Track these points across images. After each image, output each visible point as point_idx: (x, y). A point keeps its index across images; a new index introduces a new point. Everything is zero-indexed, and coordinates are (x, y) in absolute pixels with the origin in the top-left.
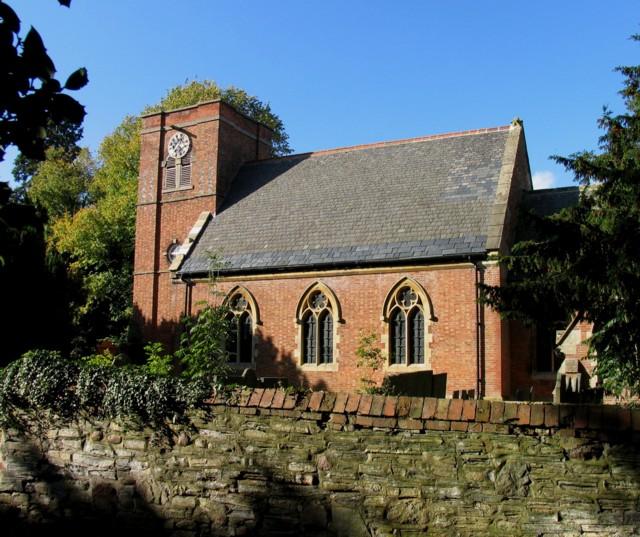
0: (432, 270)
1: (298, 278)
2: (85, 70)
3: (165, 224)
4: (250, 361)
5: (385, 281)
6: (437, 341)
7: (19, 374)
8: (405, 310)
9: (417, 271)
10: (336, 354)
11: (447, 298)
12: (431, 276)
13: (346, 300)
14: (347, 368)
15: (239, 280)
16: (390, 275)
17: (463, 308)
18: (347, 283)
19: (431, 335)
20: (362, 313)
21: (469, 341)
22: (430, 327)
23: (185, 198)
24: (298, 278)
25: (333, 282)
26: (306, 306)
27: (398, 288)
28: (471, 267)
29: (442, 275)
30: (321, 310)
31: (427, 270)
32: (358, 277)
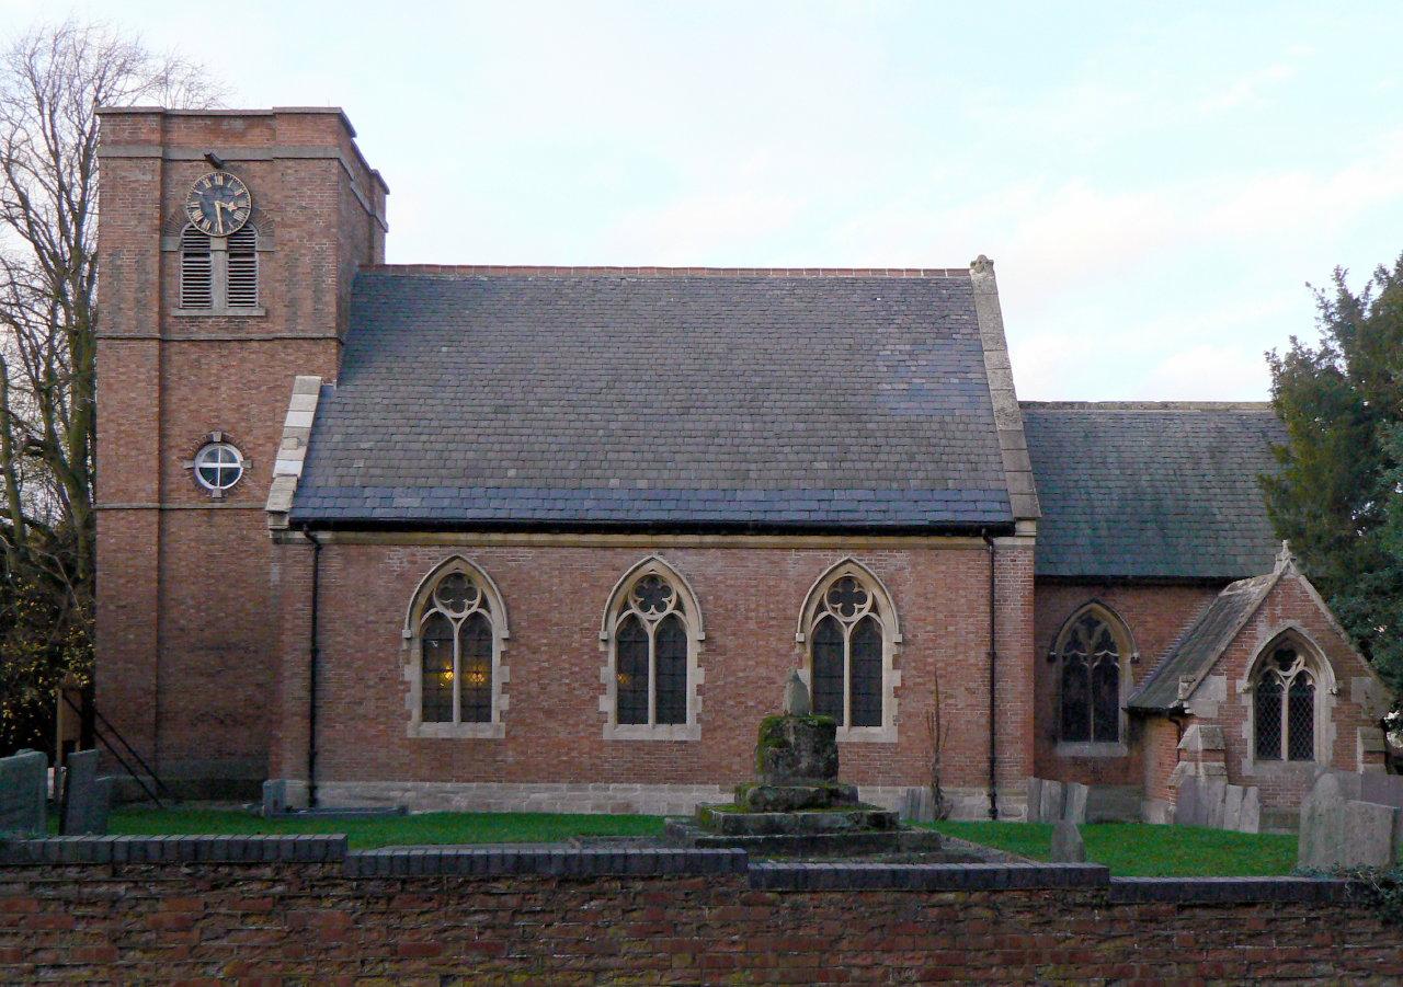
0: (899, 548)
1: (604, 547)
2: (985, 264)
3: (184, 391)
4: (488, 718)
5: (807, 568)
6: (909, 683)
7: (361, 726)
8: (847, 626)
9: (871, 549)
10: (693, 704)
11: (931, 604)
12: (899, 559)
13: (717, 598)
14: (719, 734)
15: (457, 544)
16: (811, 553)
17: (962, 625)
18: (720, 564)
19: (898, 673)
20: (752, 625)
21: (972, 685)
22: (503, 654)
23: (242, 335)
24: (604, 547)
25: (690, 560)
26: (821, 608)
27: (832, 580)
28: (980, 548)
29: (921, 560)
30: (660, 616)
31: (891, 548)
32: (744, 553)
